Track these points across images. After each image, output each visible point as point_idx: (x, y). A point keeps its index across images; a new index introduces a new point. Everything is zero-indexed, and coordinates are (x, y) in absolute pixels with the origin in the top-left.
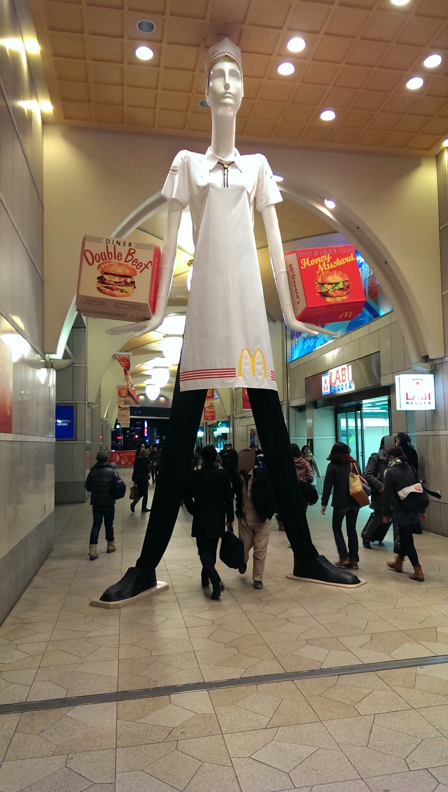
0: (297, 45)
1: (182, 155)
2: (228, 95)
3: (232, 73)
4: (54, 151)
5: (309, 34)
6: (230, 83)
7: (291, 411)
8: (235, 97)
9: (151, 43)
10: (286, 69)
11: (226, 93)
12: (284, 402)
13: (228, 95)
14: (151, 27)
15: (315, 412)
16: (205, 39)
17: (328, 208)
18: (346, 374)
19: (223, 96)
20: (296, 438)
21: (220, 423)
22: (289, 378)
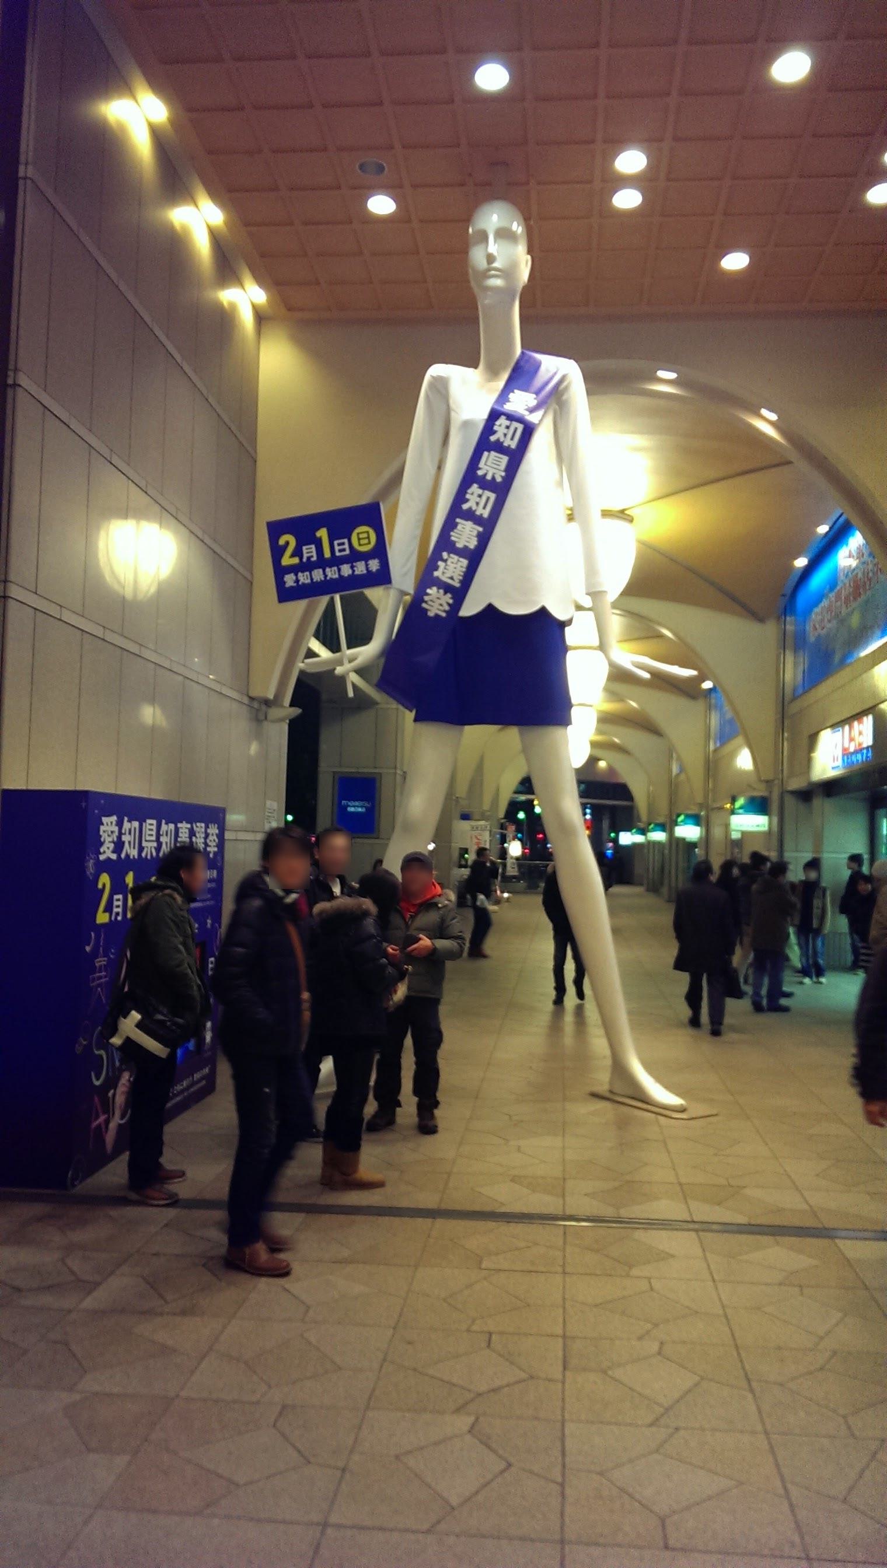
0: (631, 161)
1: (437, 370)
2: (493, 272)
3: (504, 234)
4: (278, 365)
5: (650, 143)
6: (502, 248)
7: (790, 802)
8: (508, 273)
10: (627, 199)
11: (489, 270)
12: (776, 782)
13: (493, 272)
14: (381, 169)
16: (470, 175)
17: (765, 423)
18: (864, 733)
19: (485, 274)
21: (682, 818)
22: (786, 735)
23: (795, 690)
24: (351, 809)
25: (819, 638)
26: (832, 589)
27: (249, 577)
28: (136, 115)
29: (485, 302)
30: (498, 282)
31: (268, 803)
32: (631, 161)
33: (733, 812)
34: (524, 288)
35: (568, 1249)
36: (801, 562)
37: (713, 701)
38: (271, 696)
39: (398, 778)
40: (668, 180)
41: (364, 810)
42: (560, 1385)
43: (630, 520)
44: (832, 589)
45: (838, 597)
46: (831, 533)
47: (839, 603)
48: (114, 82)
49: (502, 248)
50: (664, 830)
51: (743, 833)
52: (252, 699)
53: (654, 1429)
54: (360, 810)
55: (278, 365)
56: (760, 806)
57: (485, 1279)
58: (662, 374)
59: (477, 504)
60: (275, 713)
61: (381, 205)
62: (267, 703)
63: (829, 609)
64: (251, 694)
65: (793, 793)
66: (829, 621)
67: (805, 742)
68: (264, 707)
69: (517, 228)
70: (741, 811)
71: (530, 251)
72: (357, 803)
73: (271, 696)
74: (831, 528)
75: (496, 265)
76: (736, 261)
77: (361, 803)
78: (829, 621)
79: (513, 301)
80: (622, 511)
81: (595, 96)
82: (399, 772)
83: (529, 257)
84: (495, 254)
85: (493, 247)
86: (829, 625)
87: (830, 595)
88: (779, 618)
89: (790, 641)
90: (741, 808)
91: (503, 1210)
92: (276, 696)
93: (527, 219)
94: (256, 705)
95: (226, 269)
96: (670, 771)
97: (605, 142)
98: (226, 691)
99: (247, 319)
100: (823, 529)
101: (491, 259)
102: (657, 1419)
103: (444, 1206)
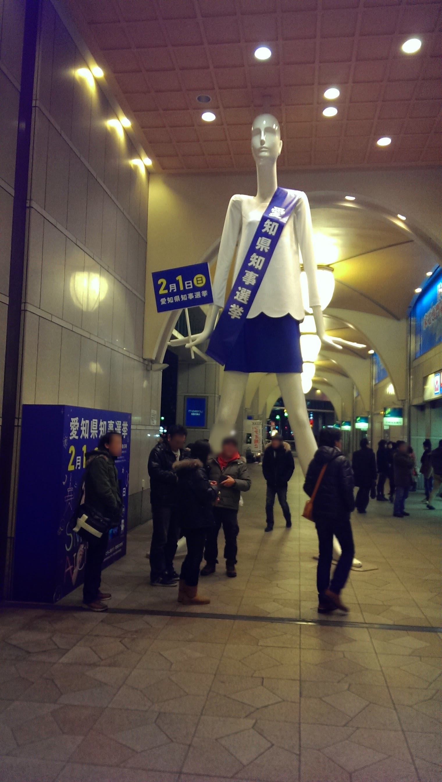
0: (332, 93)
1: (236, 197)
3: (269, 130)
4: (158, 196)
5: (341, 85)
6: (268, 137)
7: (414, 410)
8: (271, 149)
9: (214, 109)
10: (330, 112)
11: (262, 148)
12: (407, 401)
15: (433, 411)
17: (400, 222)
19: (260, 150)
20: (419, 437)
21: (359, 419)
22: (411, 377)
23: (416, 354)
24: (194, 414)
25: (427, 328)
26: (434, 304)
27: (143, 299)
28: (89, 75)
29: (260, 163)
30: (266, 154)
31: (152, 411)
32: (332, 93)
33: (385, 416)
34: (279, 157)
35: (302, 636)
36: (418, 290)
37: (374, 360)
38: (154, 358)
39: (216, 399)
40: (351, 102)
41: (199, 414)
42: (298, 704)
43: (332, 270)
44: (434, 304)
45: (438, 307)
46: (434, 276)
47: (438, 311)
48: (79, 60)
49: (268, 137)
50: (350, 425)
51: (390, 426)
52: (145, 360)
53: (345, 728)
54: (197, 414)
55: (158, 196)
56: (398, 412)
57: (260, 650)
58: (348, 198)
59: (256, 263)
60: (155, 366)
61: (209, 117)
62: (152, 361)
63: (433, 314)
64: (144, 357)
65: (415, 406)
66: (433, 320)
67: (421, 380)
68: (150, 364)
69: (275, 127)
70: (389, 415)
71: (282, 139)
72: (196, 411)
73: (154, 358)
74: (433, 274)
75: (264, 146)
76: (384, 142)
77: (198, 411)
78: (433, 320)
79: (273, 164)
80: (328, 266)
81: (314, 62)
82: (217, 395)
83: (281, 141)
84: (264, 140)
85: (263, 137)
86: (433, 322)
87: (434, 307)
88: (407, 319)
89: (413, 330)
90: (389, 414)
91: (269, 616)
92: (156, 358)
93: (280, 123)
94: (146, 362)
95: (133, 149)
96: (353, 395)
97: (319, 84)
98: (132, 356)
99: (143, 173)
100: (429, 274)
101: (262, 142)
102: (348, 723)
103: (240, 614)
